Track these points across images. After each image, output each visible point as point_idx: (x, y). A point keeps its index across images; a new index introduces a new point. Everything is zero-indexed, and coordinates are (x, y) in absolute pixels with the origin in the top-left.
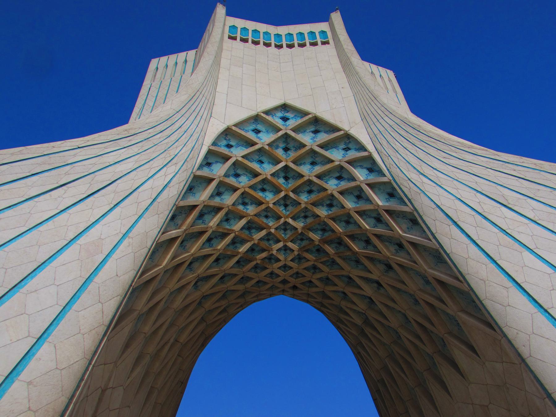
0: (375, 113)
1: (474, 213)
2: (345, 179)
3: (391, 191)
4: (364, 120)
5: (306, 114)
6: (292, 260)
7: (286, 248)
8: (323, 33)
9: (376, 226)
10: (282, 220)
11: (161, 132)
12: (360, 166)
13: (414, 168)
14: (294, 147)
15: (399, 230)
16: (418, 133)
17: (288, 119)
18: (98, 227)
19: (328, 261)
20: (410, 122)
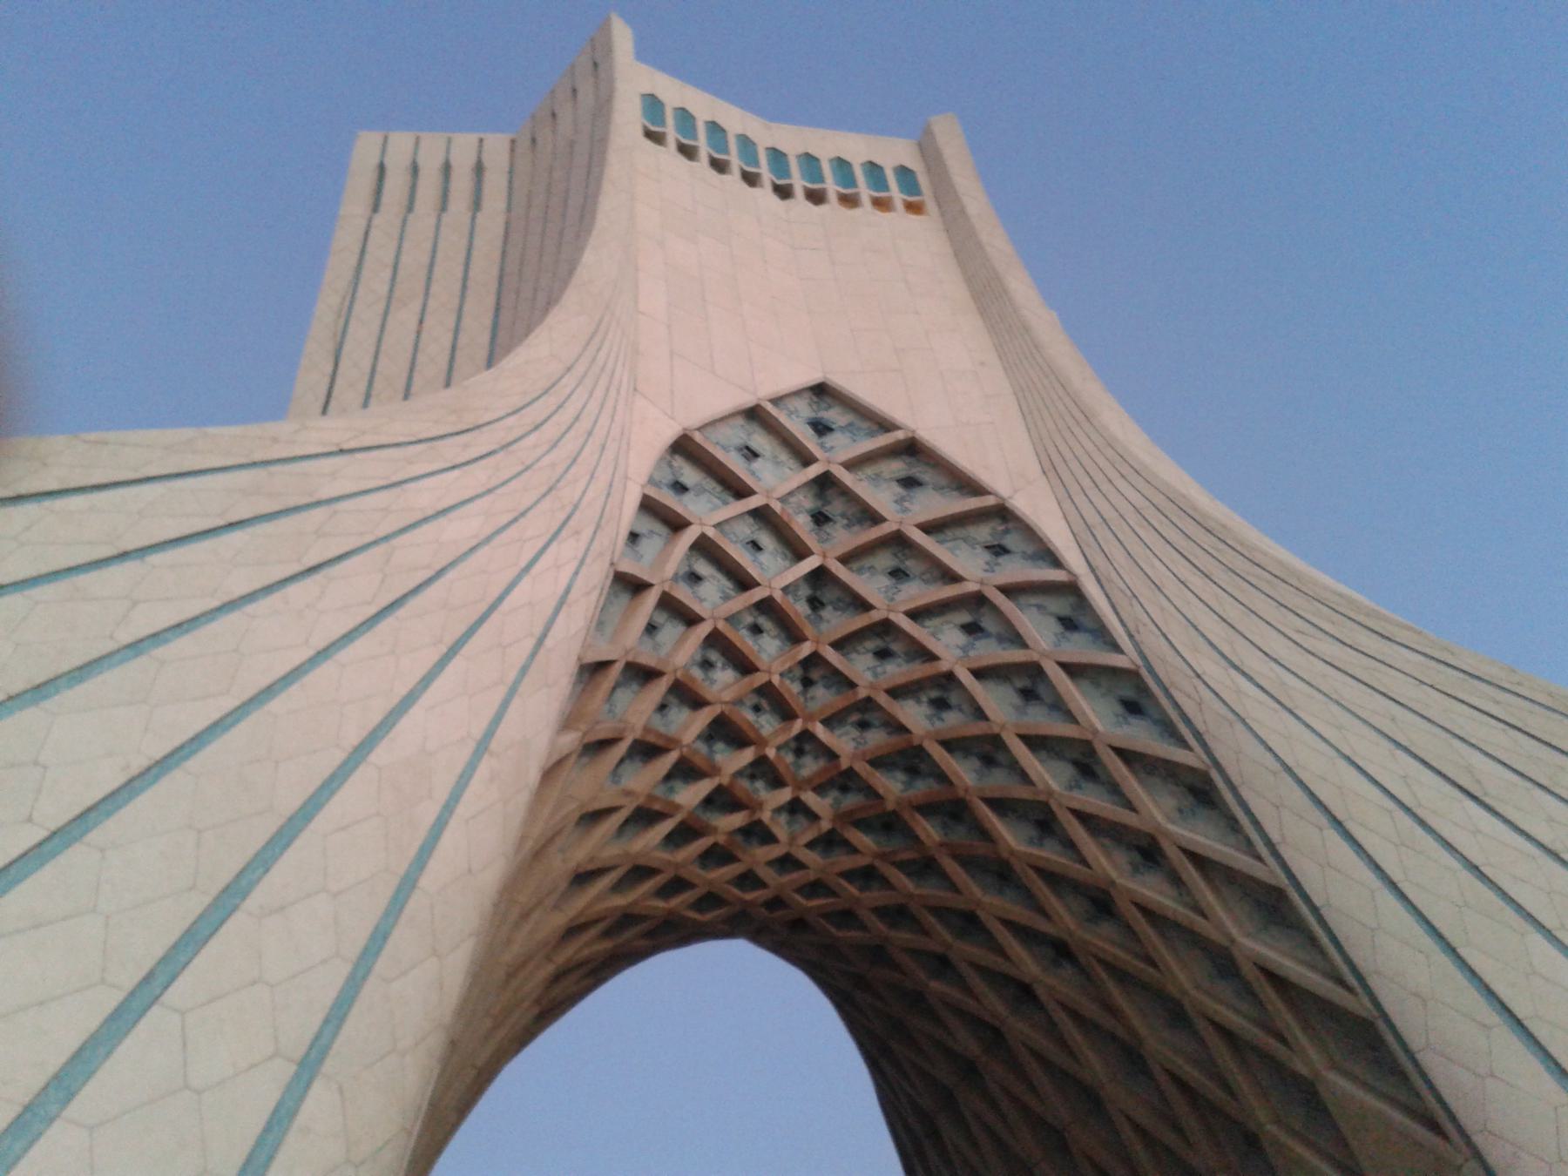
0: (1085, 460)
1: (1390, 804)
2: (988, 635)
3: (1135, 693)
4: (1051, 474)
5: (885, 425)
6: (810, 845)
7: (795, 808)
8: (904, 173)
9: (1080, 788)
10: (798, 726)
11: (537, 428)
12: (1039, 607)
13: (1211, 644)
14: (843, 515)
15: (1157, 810)
16: (1222, 546)
17: (830, 430)
18: (416, 713)
19: (913, 861)
20: (1195, 509)
